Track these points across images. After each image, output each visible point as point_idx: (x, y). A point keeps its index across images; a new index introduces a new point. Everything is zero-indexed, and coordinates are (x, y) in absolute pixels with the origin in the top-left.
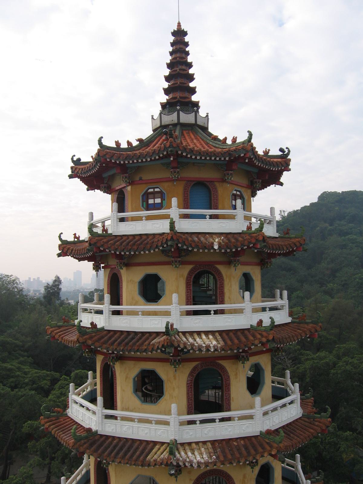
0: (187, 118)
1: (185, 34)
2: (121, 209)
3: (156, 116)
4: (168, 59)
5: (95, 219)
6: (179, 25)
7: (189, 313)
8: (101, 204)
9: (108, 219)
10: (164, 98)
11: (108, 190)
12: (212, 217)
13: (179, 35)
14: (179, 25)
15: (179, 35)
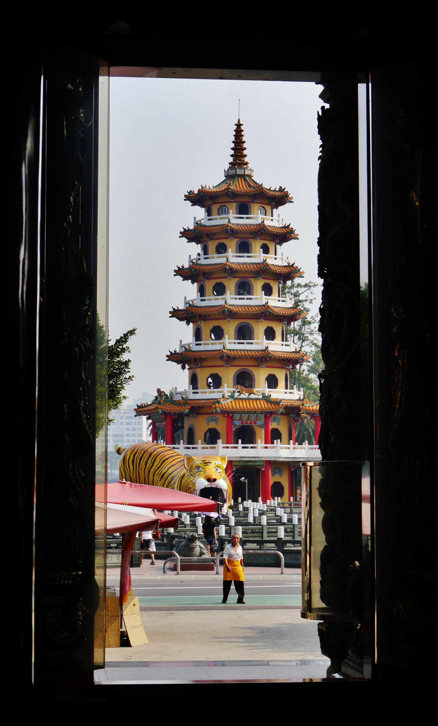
0: (239, 172)
1: (242, 125)
2: (209, 215)
3: (226, 170)
4: (233, 139)
5: (197, 220)
6: (239, 120)
7: (237, 256)
8: (200, 213)
9: (203, 219)
10: (231, 160)
11: (202, 206)
12: (247, 218)
13: (239, 125)
14: (239, 120)
15: (239, 125)
